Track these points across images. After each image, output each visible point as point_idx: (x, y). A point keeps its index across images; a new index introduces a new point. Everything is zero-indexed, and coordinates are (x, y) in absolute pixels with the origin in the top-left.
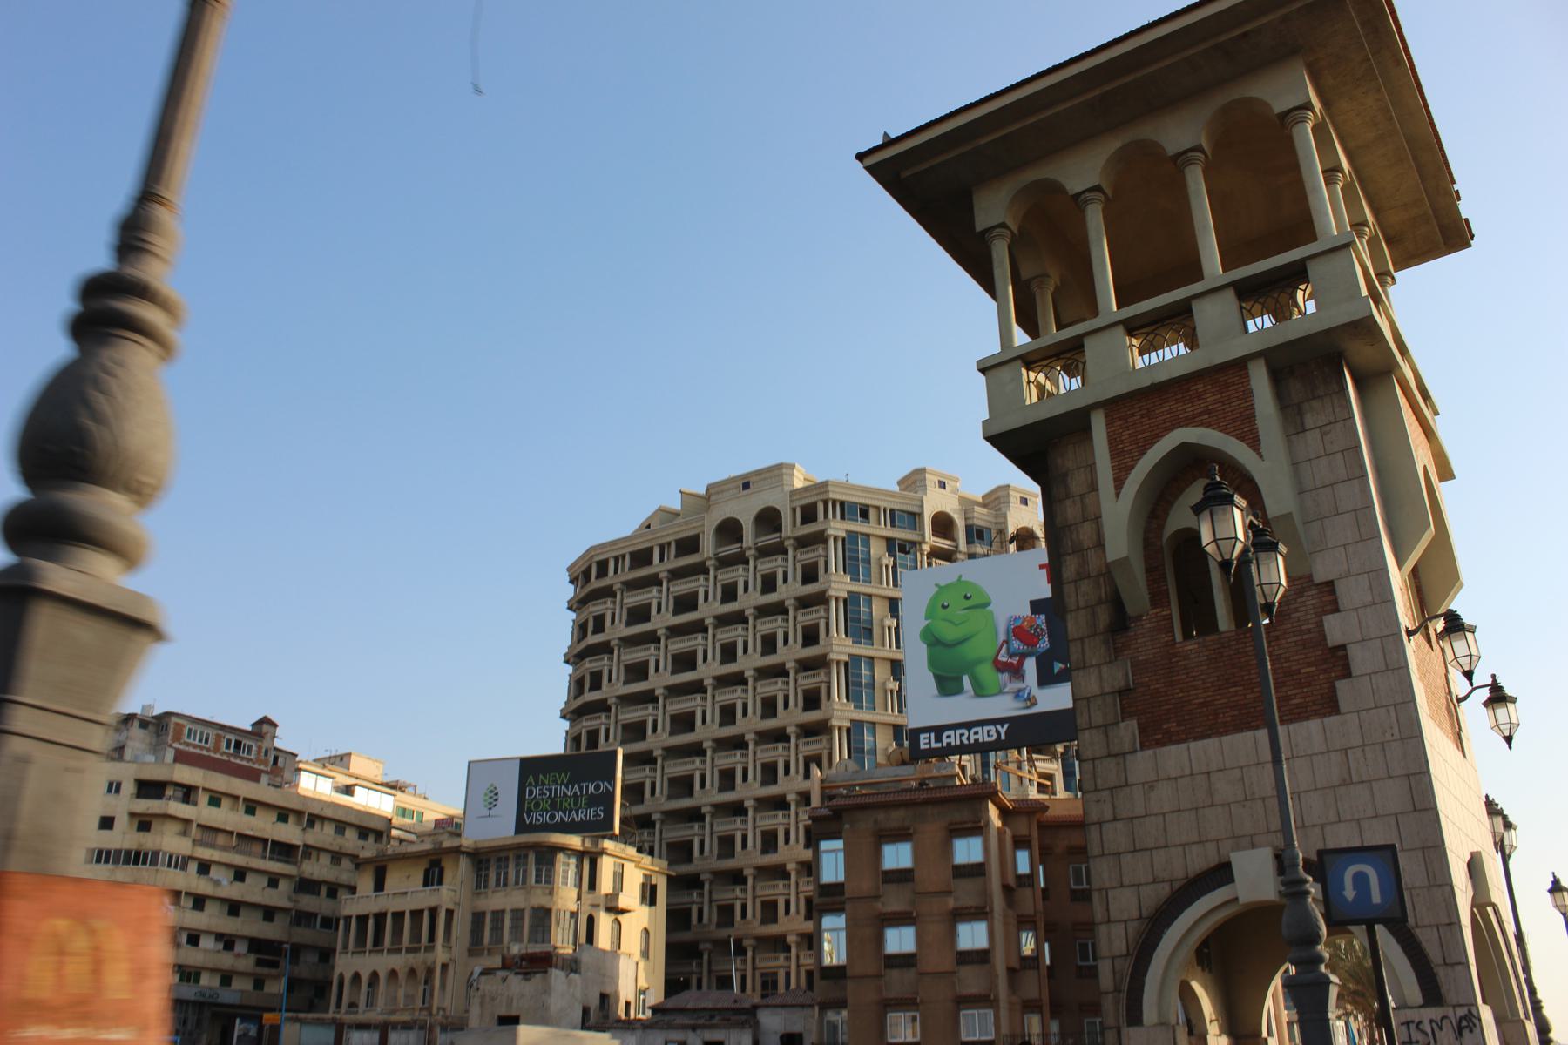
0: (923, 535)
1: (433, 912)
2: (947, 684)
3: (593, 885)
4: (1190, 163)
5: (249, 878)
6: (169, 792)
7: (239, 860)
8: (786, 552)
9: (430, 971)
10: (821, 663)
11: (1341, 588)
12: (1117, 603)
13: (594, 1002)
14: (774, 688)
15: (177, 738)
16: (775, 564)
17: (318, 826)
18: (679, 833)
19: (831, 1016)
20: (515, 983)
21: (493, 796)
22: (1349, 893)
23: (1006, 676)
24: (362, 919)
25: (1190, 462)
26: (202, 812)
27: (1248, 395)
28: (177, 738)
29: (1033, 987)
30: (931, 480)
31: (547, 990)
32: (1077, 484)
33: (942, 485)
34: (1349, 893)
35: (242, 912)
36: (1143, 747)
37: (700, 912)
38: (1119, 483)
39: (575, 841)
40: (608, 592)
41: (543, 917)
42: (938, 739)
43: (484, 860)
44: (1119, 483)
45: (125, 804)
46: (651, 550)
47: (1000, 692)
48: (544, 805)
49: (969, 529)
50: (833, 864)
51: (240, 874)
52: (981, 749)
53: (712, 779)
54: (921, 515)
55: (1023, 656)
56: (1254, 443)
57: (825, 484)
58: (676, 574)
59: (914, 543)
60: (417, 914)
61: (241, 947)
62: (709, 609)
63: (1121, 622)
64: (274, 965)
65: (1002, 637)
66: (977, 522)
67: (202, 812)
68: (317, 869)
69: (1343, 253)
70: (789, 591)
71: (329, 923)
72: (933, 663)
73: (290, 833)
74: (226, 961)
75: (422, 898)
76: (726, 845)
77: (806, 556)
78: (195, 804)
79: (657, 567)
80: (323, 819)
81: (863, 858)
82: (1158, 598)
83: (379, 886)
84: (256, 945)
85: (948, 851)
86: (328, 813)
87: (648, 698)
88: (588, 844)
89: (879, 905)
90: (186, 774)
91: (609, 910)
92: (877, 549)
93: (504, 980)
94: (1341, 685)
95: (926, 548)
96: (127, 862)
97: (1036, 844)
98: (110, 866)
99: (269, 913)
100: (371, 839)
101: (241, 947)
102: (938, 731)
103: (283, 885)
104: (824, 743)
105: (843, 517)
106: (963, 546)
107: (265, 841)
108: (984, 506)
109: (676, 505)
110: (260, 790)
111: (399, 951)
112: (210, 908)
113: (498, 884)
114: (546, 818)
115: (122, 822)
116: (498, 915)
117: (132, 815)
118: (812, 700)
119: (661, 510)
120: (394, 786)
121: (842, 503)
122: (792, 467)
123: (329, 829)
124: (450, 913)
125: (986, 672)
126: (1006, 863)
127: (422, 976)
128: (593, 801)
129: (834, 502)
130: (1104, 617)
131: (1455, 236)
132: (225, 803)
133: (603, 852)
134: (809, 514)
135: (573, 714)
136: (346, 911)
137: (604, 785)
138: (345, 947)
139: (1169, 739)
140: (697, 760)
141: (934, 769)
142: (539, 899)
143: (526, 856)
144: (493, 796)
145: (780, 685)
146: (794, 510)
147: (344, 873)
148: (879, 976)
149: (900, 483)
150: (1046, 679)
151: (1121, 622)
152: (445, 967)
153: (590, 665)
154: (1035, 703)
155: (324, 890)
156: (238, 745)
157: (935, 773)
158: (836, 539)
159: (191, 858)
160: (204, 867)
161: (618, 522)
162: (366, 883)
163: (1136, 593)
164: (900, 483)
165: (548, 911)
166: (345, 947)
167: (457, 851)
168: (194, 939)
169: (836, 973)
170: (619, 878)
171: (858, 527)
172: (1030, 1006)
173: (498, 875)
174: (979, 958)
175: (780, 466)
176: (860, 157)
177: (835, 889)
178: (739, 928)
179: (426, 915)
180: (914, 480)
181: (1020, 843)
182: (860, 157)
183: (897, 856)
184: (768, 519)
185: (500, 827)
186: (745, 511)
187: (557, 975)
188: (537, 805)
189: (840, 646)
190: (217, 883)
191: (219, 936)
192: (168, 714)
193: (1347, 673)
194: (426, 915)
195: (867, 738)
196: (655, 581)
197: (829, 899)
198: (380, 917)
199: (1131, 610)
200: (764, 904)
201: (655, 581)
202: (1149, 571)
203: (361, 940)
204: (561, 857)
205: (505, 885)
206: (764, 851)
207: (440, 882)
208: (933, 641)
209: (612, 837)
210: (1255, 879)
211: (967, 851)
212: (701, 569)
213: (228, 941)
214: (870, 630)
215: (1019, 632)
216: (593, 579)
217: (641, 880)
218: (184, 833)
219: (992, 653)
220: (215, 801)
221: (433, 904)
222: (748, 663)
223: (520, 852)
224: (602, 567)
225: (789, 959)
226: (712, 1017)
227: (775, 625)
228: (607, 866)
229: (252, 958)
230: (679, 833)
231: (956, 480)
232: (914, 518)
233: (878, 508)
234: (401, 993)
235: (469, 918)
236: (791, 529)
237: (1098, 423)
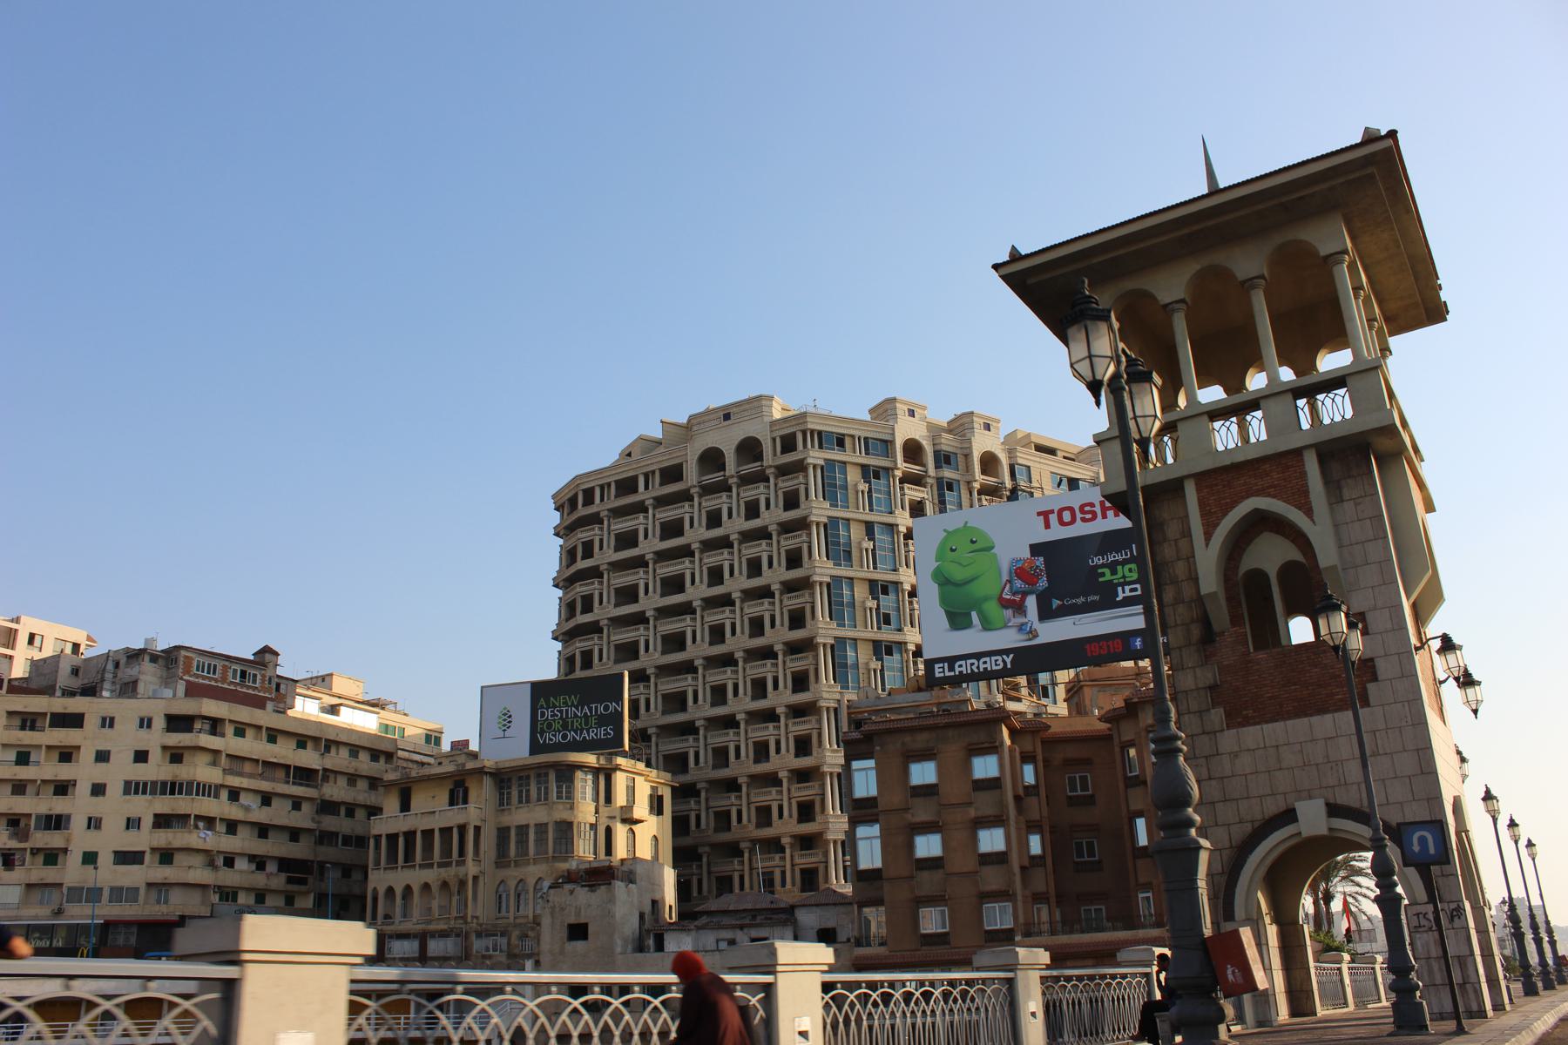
0: (895, 462)
1: (462, 829)
2: (958, 620)
3: (609, 800)
4: (1254, 287)
5: (275, 802)
6: (198, 725)
7: (265, 786)
8: (767, 480)
9: (462, 883)
10: (805, 584)
11: (1369, 617)
12: (1206, 622)
13: (647, 909)
14: (761, 608)
15: (187, 671)
16: (758, 492)
17: (333, 750)
18: (675, 746)
19: (868, 911)
20: (582, 895)
21: (507, 719)
22: (1416, 848)
23: (1010, 612)
24: (392, 838)
25: (1260, 522)
26: (229, 743)
27: (1303, 475)
28: (187, 671)
29: (1040, 882)
30: (901, 409)
31: (612, 900)
32: (1172, 531)
33: (912, 413)
34: (1416, 848)
35: (270, 834)
36: (1228, 728)
37: (698, 817)
38: (1208, 536)
39: (590, 759)
40: (595, 519)
41: (566, 830)
42: (951, 669)
43: (504, 778)
44: (1208, 536)
45: (156, 738)
46: (635, 478)
47: (1006, 626)
48: (556, 726)
49: (937, 454)
50: (865, 782)
51: (267, 799)
52: (987, 676)
53: (705, 696)
54: (892, 442)
55: (1025, 594)
56: (1309, 512)
57: (803, 415)
58: (661, 502)
59: (887, 469)
60: (446, 832)
61: (271, 867)
62: (695, 534)
63: (1208, 637)
64: (302, 882)
65: (1005, 577)
66: (944, 448)
67: (229, 743)
68: (336, 791)
69: (1373, 373)
70: (772, 516)
71: (361, 841)
72: (945, 601)
73: (309, 758)
74: (260, 880)
75: (453, 817)
76: (721, 756)
77: (787, 484)
78: (223, 735)
79: (642, 495)
80: (338, 744)
81: (892, 776)
82: (1236, 620)
83: (405, 806)
84: (285, 864)
85: (968, 768)
86: (343, 738)
87: (640, 619)
88: (602, 761)
89: (909, 817)
90: (211, 707)
91: (624, 821)
92: (853, 475)
93: (572, 892)
94: (1371, 687)
95: (898, 473)
96: (163, 793)
97: (1040, 758)
98: (148, 797)
99: (294, 834)
100: (382, 760)
101: (271, 867)
102: (951, 661)
103: (305, 807)
104: (810, 660)
105: (821, 447)
106: (932, 471)
107: (288, 767)
108: (950, 431)
109: (657, 433)
110: (266, 717)
111: (431, 866)
112: (243, 832)
113: (520, 802)
114: (559, 738)
115: (156, 755)
116: (523, 830)
117: (165, 748)
118: (797, 620)
119: (641, 438)
120: (375, 705)
121: (820, 433)
122: (771, 398)
123: (344, 752)
124: (477, 829)
125: (992, 608)
126: (1017, 776)
127: (455, 889)
128: (603, 721)
129: (812, 432)
130: (1196, 631)
131: (1435, 313)
132: (250, 733)
133: (617, 768)
134: (788, 444)
135: (566, 635)
136: (375, 832)
137: (613, 706)
138: (377, 863)
139: (1247, 722)
140: (689, 677)
141: (949, 695)
142: (560, 814)
143: (546, 775)
144: (507, 719)
145: (766, 606)
146: (774, 440)
147: (360, 794)
148: (912, 877)
149: (871, 411)
150: (1046, 614)
151: (1208, 637)
152: (475, 878)
153: (581, 589)
154: (1036, 636)
155: (343, 811)
156: (243, 674)
157: (949, 699)
158: (815, 467)
159: (222, 786)
160: (234, 794)
161: (599, 453)
162: (391, 804)
163: (1220, 616)
164: (871, 411)
165: (571, 824)
166: (377, 863)
167: (481, 772)
168: (229, 862)
169: (872, 876)
170: (631, 790)
171: (836, 455)
172: (1038, 898)
173: (520, 792)
174: (998, 858)
175: (759, 398)
176: (996, 267)
177: (869, 802)
178: (736, 833)
179: (455, 831)
180: (885, 410)
181: (1027, 758)
182: (996, 267)
183: (923, 773)
184: (750, 449)
185: (516, 749)
186: (727, 440)
187: (619, 886)
188: (550, 726)
189: (822, 568)
190: (247, 809)
191: (252, 858)
192: (178, 648)
193: (1375, 678)
194: (455, 831)
195: (850, 653)
196: (640, 508)
197: (862, 811)
198: (410, 835)
199: (1216, 627)
200: (758, 808)
201: (640, 508)
202: (1229, 599)
203: (392, 857)
204: (579, 775)
205: (528, 801)
206: (757, 761)
207: (465, 801)
208: (944, 581)
209: (624, 755)
210: (1312, 819)
211: (985, 767)
212: (685, 496)
213: (259, 862)
214: (849, 553)
215: (1020, 572)
216: (579, 507)
217: (649, 792)
218: (214, 763)
219: (997, 591)
220: (240, 732)
221: (461, 822)
222: (735, 584)
223: (541, 771)
224: (589, 495)
225: (783, 859)
226: (754, 917)
227: (760, 549)
228: (620, 780)
229: (283, 876)
230: (675, 746)
231: (924, 408)
232: (887, 445)
233: (853, 436)
234: (435, 904)
235: (494, 833)
236: (771, 458)
237: (1190, 490)
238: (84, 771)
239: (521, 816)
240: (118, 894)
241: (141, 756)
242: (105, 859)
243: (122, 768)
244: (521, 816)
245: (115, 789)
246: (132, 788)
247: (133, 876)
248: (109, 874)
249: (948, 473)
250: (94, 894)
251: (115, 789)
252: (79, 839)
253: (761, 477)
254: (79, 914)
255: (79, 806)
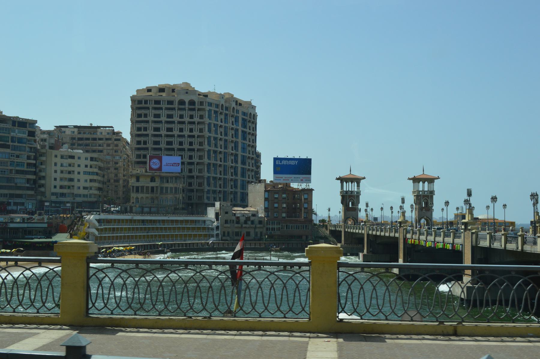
45: (89, 163)
116: (167, 188)
134: (201, 103)
171: (211, 108)
184: (192, 103)
236: (197, 106)
238: (76, 169)
239: (166, 185)
240: (84, 196)
241: (86, 166)
242: (81, 188)
243: (82, 169)
244: (166, 185)
245: (82, 173)
246: (85, 173)
247: (86, 192)
248: (82, 192)
249: (227, 112)
250: (80, 196)
251: (82, 173)
252: (76, 183)
253: (194, 110)
254: (79, 200)
255: (75, 176)
